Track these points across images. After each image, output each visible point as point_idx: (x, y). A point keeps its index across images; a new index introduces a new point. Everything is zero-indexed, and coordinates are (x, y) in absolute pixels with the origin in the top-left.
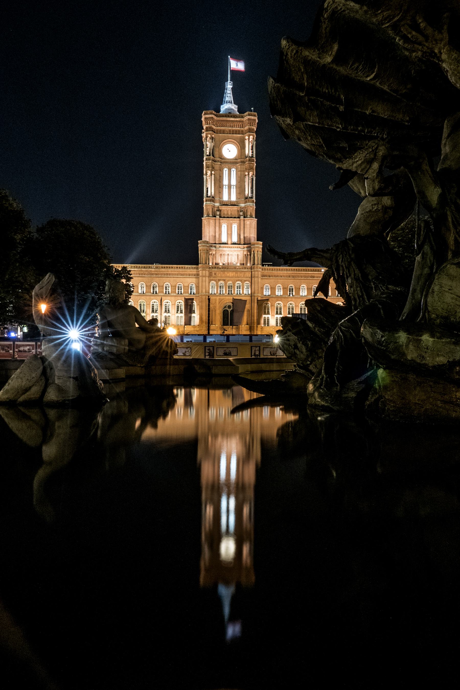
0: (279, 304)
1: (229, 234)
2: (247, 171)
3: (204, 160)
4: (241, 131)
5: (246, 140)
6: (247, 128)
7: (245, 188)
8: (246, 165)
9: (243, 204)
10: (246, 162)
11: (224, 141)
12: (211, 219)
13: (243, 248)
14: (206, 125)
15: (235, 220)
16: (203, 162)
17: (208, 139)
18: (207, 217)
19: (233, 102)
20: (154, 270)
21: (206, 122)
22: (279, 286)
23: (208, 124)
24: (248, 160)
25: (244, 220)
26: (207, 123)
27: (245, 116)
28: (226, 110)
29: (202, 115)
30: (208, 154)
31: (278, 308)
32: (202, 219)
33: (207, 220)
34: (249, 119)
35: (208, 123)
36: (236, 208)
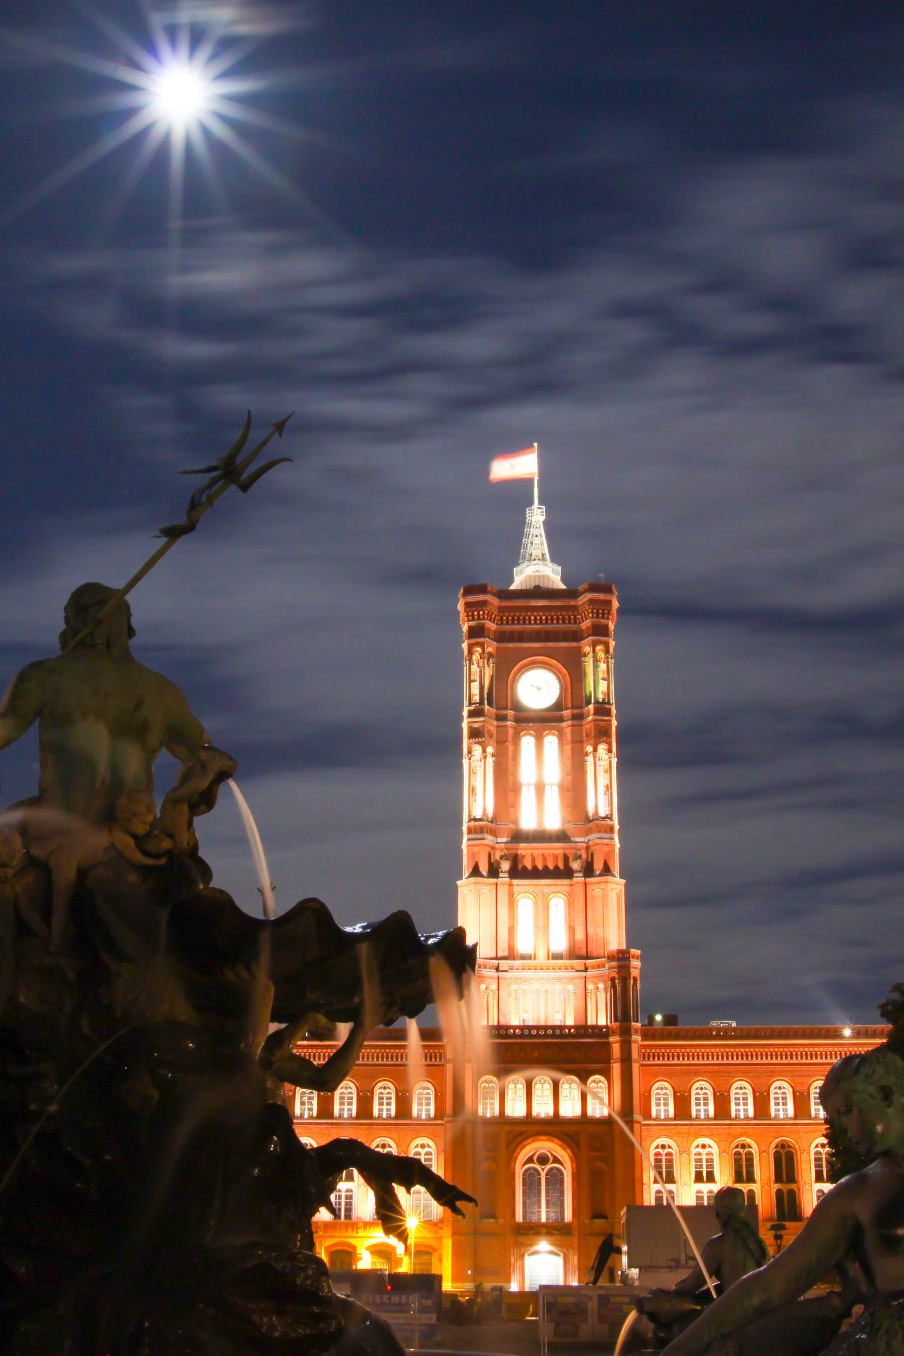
0: (703, 1146)
1: (543, 926)
3: (462, 717)
6: (586, 624)
10: (587, 717)
12: (484, 884)
13: (583, 968)
14: (468, 620)
15: (556, 885)
16: (463, 720)
17: (474, 658)
18: (472, 880)
19: (548, 557)
20: (305, 1043)
22: (701, 1089)
23: (473, 619)
24: (592, 711)
25: (585, 884)
26: (473, 615)
27: (582, 593)
29: (459, 596)
30: (476, 698)
31: (700, 1160)
32: (456, 887)
33: (472, 887)
34: (591, 601)
35: (476, 617)
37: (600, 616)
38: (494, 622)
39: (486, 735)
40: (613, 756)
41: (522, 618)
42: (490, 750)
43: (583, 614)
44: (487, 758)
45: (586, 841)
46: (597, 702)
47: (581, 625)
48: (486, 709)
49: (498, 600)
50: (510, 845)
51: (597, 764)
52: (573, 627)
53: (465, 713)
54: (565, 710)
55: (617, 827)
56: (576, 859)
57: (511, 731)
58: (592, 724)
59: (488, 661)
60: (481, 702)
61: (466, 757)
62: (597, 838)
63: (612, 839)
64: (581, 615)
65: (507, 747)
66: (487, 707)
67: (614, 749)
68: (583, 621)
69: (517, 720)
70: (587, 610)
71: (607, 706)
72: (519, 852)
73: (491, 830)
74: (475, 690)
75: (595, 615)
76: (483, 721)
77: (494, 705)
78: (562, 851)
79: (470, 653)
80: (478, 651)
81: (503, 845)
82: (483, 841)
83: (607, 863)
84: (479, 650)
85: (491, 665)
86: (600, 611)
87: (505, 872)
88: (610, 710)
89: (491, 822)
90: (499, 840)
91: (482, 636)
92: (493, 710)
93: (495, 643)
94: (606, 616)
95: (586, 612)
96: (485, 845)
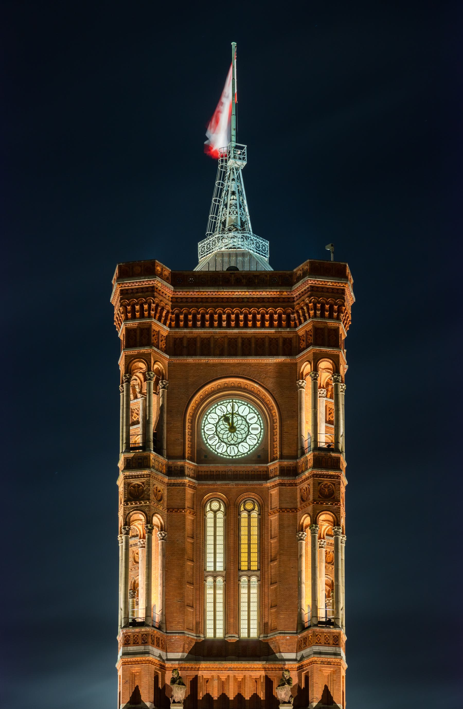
2: (310, 508)
3: (118, 468)
4: (281, 341)
5: (302, 377)
7: (299, 584)
8: (305, 485)
9: (292, 652)
10: (303, 472)
11: (208, 387)
14: (127, 319)
16: (118, 475)
21: (125, 307)
24: (311, 464)
28: (219, 259)
29: (113, 282)
30: (137, 439)
35: (138, 314)
36: (259, 669)
37: (327, 313)
38: (165, 324)
39: (152, 497)
40: (341, 531)
41: (207, 316)
42: (157, 520)
43: (300, 311)
44: (154, 531)
45: (298, 659)
46: (316, 448)
47: (297, 329)
48: (152, 457)
49: (172, 288)
50: (187, 665)
51: (318, 545)
52: (285, 332)
53: (121, 464)
54: (271, 462)
55: (344, 638)
56: (283, 684)
57: (189, 492)
58: (311, 481)
59: (156, 383)
60: (145, 447)
61: (123, 530)
62: (315, 653)
63: (337, 654)
64: (297, 312)
65: (184, 516)
66: (153, 455)
67: (343, 521)
68: (300, 323)
69: (199, 477)
70: (307, 305)
71: (333, 454)
72: (200, 673)
73: (158, 639)
74: (137, 430)
75: (318, 312)
76: (149, 476)
77: (165, 452)
78: (263, 673)
79: (129, 371)
80: (141, 368)
81: (177, 662)
82: (147, 655)
83: (328, 690)
84: (142, 365)
85: (161, 390)
86: (327, 306)
87: (179, 702)
88: (338, 460)
89: (159, 628)
90: (171, 655)
91: (149, 344)
92: (163, 460)
93: (168, 357)
94: (335, 314)
95: (305, 308)
96: (150, 662)
